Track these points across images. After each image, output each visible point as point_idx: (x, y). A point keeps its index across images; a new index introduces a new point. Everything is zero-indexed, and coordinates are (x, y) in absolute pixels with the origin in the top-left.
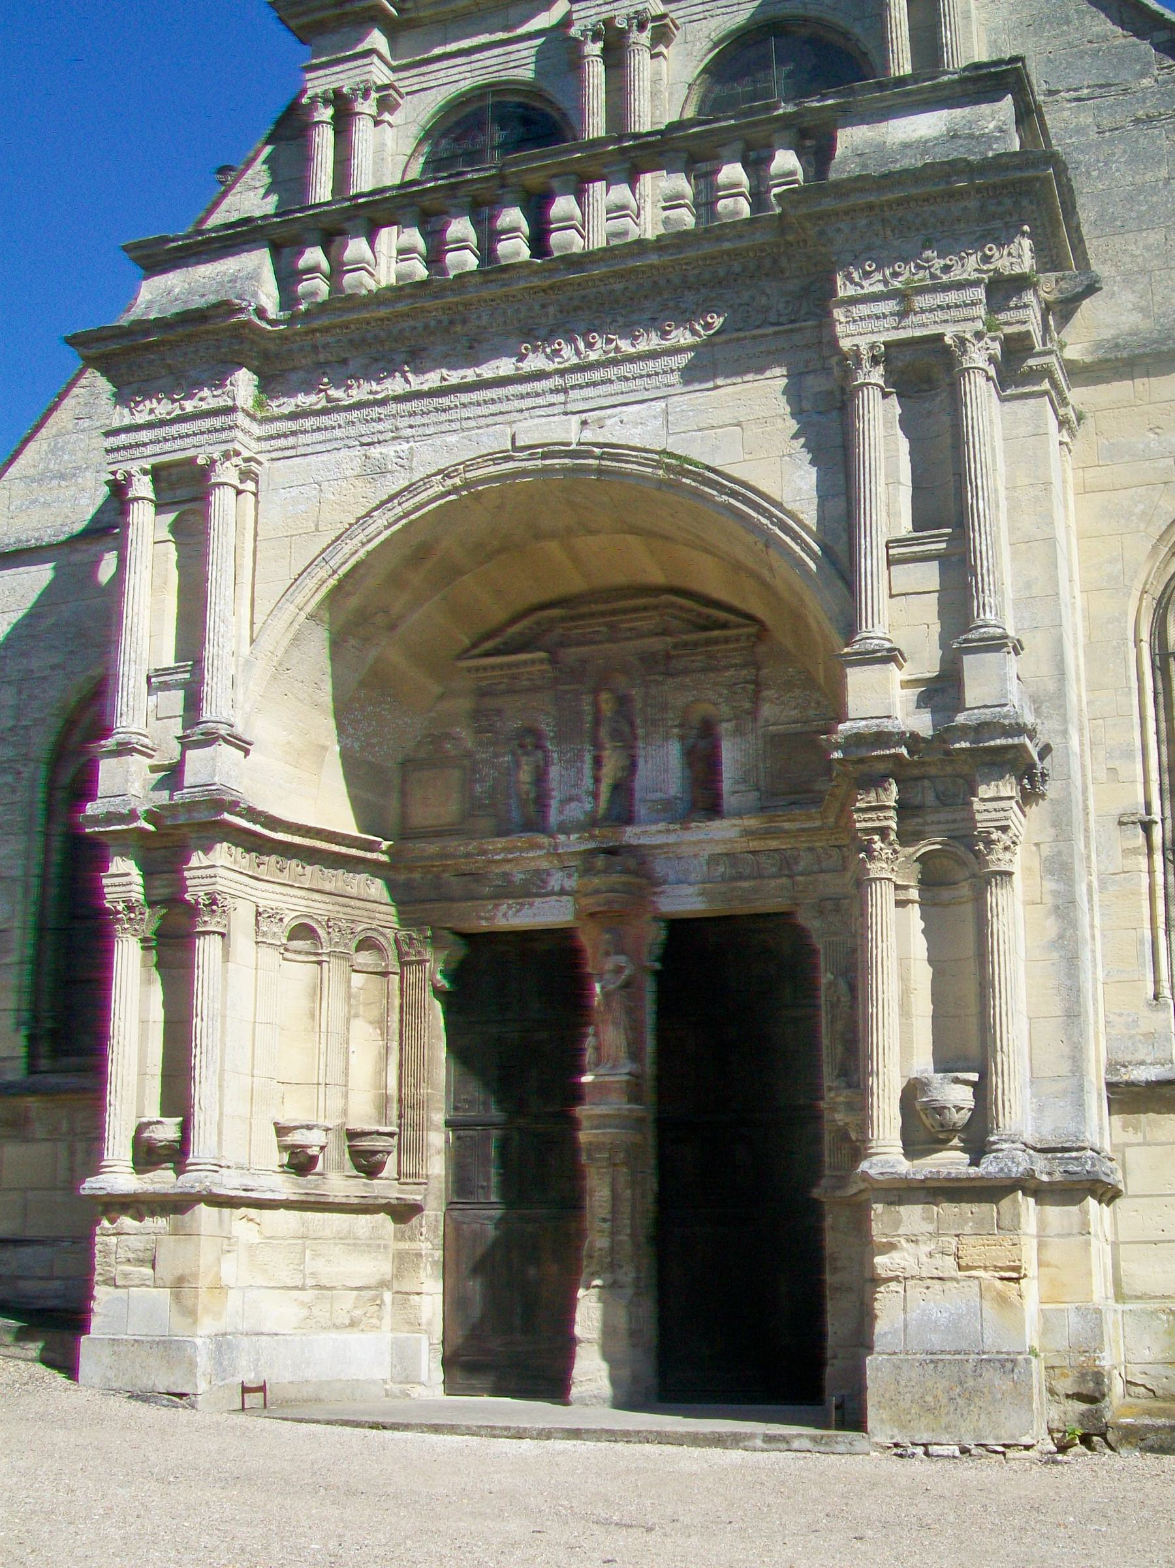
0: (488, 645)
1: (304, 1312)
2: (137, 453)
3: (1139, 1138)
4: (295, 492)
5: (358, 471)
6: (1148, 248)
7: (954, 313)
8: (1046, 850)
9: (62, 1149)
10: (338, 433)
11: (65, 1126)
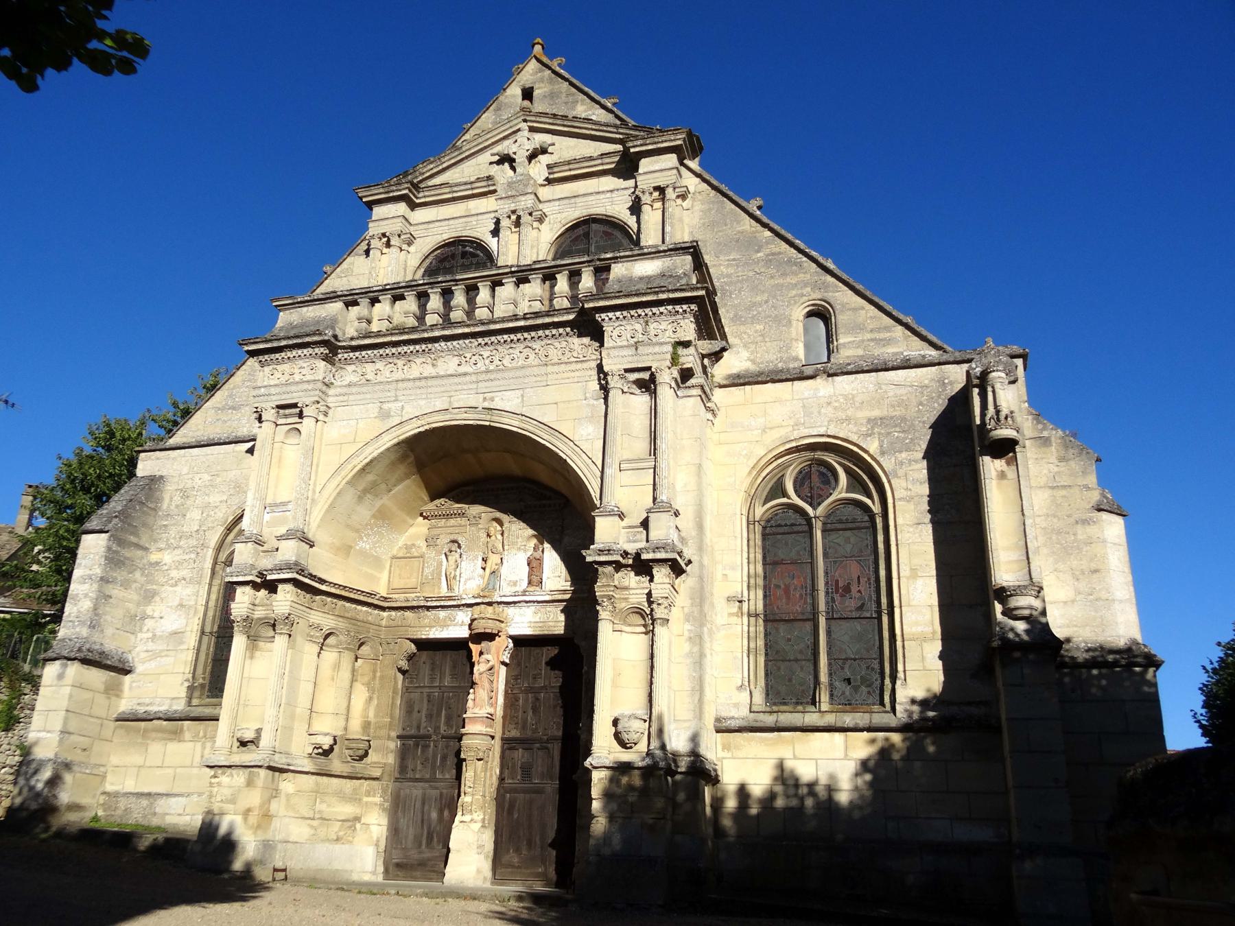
1: (312, 832)
2: (269, 398)
3: (729, 755)
6: (756, 332)
7: (658, 357)
8: (686, 610)
9: (199, 745)
10: (368, 396)
11: (201, 734)
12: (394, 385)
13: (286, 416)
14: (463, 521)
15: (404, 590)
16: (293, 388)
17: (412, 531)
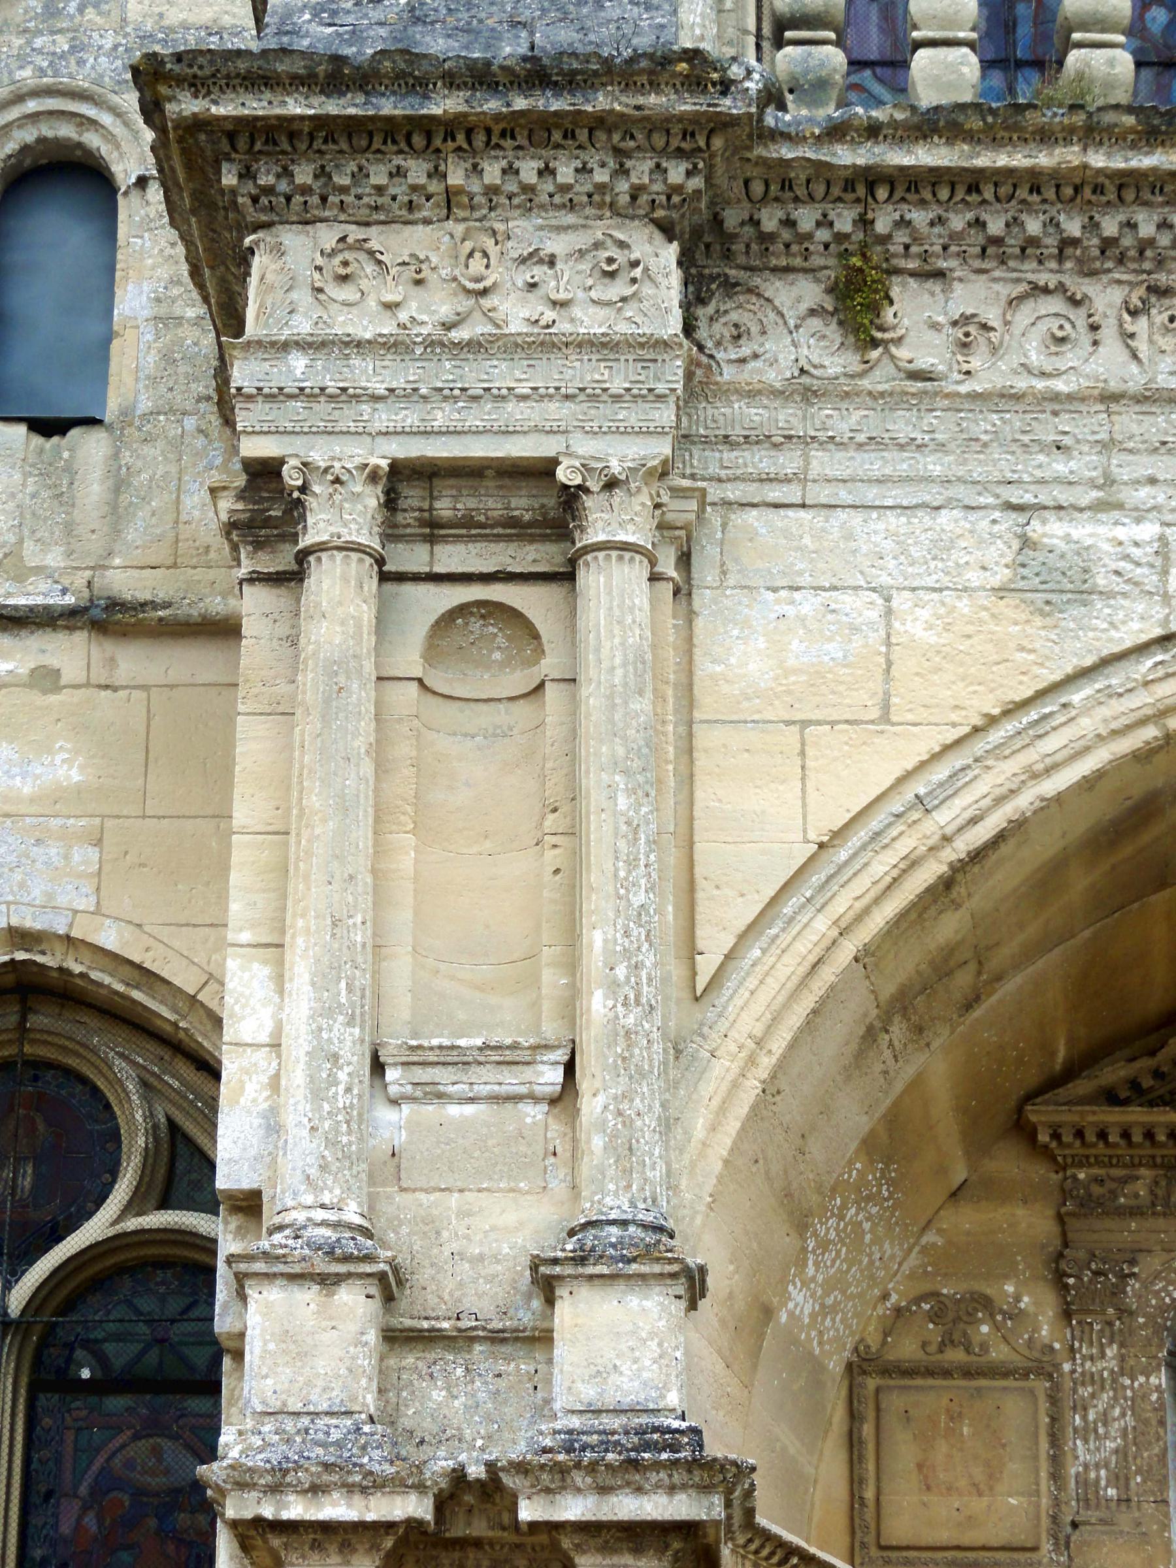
0: (1114, 1073)
2: (346, 417)
4: (808, 604)
5: (1002, 575)
10: (934, 465)
12: (1087, 425)
13: (433, 531)
16: (502, 373)
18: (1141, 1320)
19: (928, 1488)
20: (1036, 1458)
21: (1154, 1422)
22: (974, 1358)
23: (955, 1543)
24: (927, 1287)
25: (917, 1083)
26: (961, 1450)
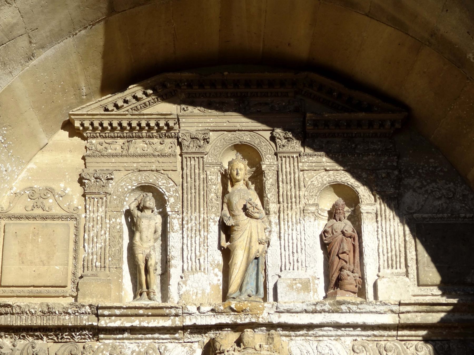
14: (169, 145)
15: (36, 290)
17: (42, 159)
18: (115, 197)
19: (23, 263)
20: (68, 250)
21: (118, 237)
22: (45, 212)
23: (32, 284)
24: (29, 185)
25: (9, 89)
26: (37, 248)
